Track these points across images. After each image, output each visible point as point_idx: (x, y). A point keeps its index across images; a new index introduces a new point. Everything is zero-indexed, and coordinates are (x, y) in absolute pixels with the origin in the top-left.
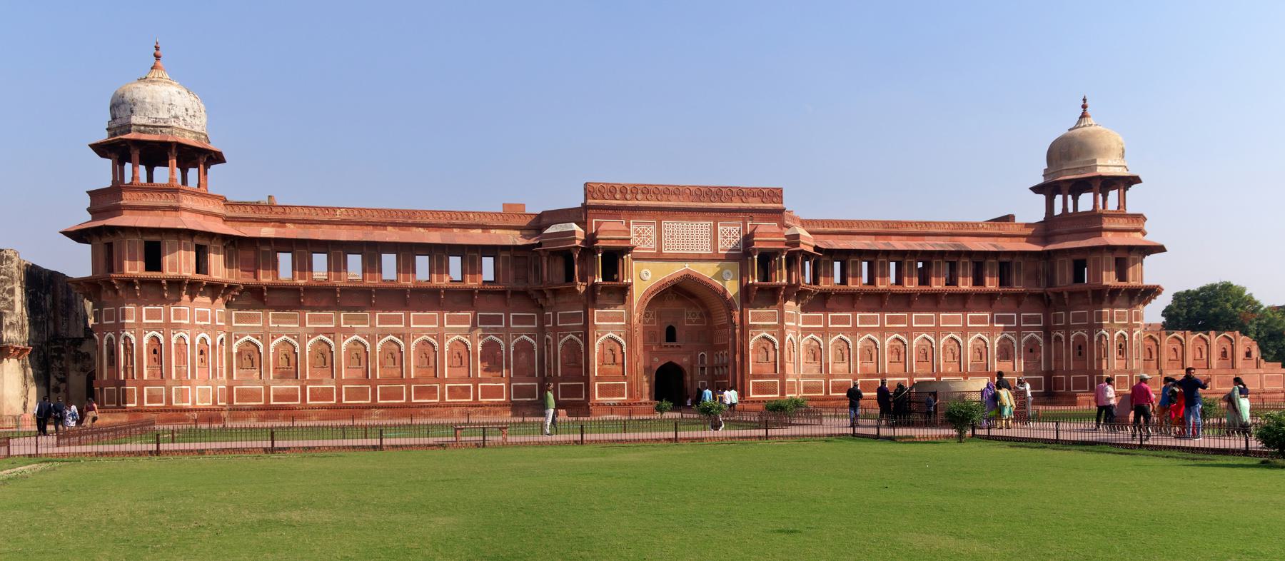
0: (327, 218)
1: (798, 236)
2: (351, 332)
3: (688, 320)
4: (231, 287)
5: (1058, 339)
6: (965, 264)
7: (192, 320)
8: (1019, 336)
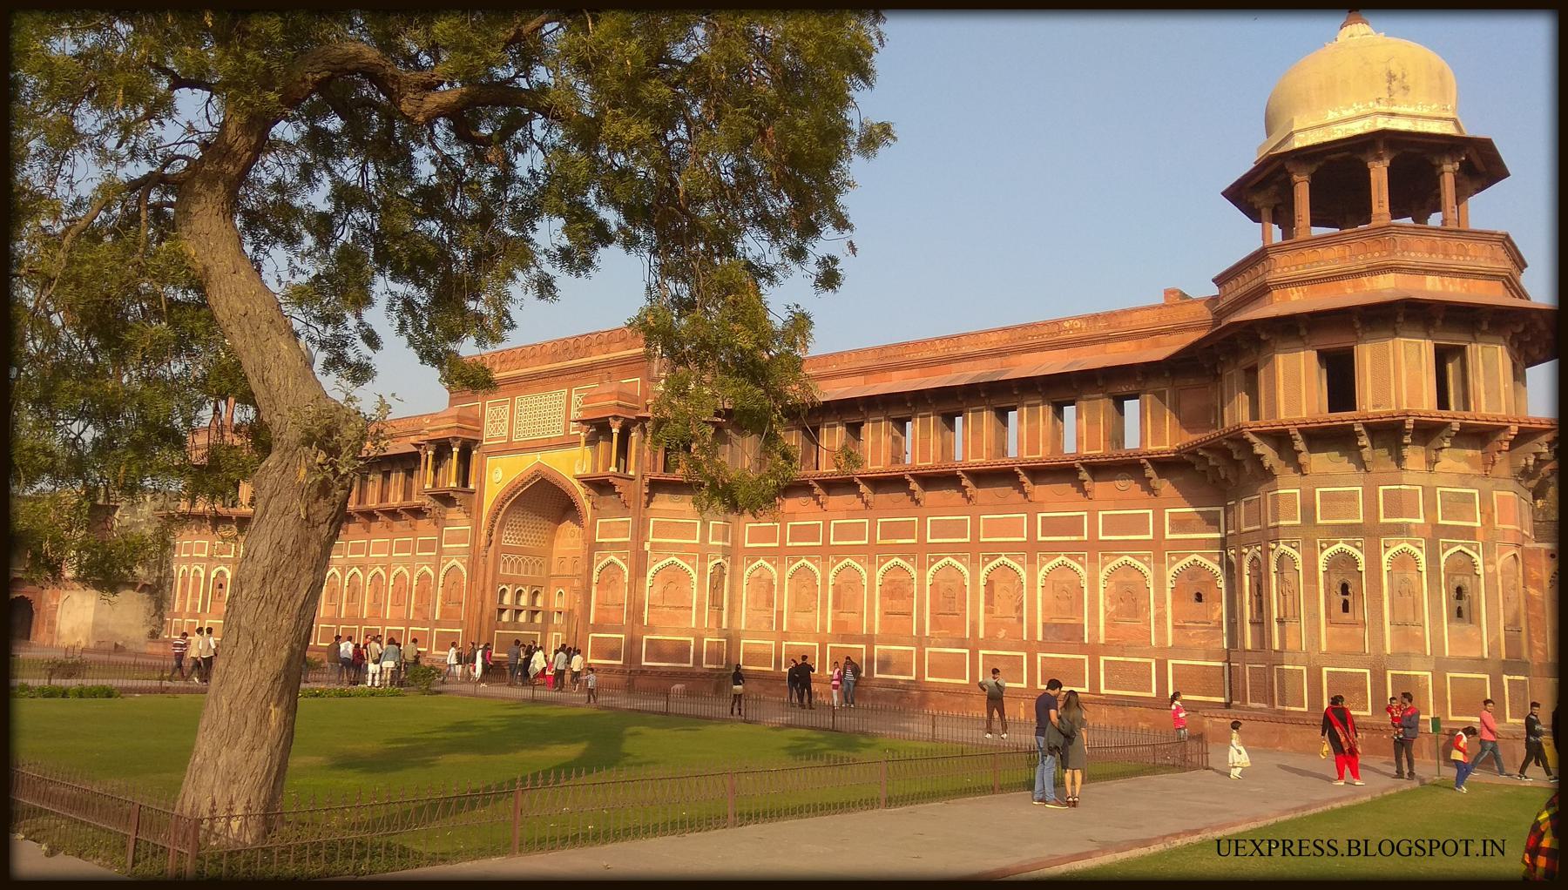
8: (1159, 560)
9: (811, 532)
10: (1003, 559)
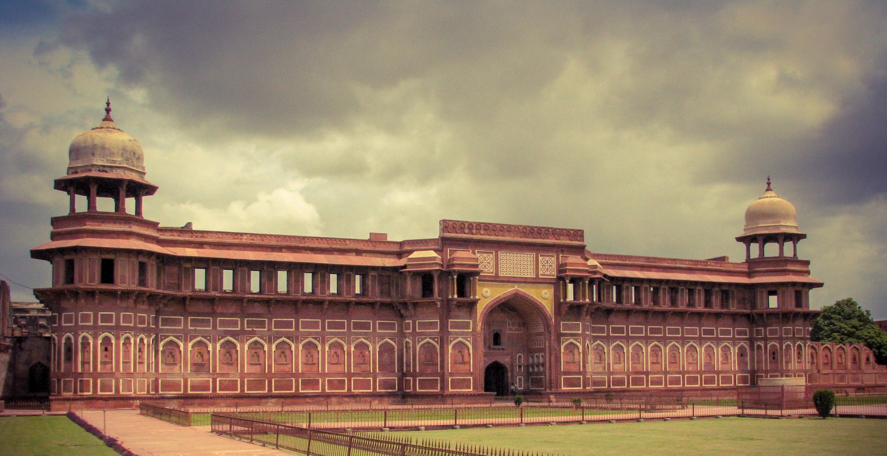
0: (236, 241)
1: (596, 266)
2: (253, 333)
3: (510, 330)
4: (165, 296)
5: (759, 347)
6: (699, 291)
7: (135, 324)
9: (621, 330)
10: (692, 343)
